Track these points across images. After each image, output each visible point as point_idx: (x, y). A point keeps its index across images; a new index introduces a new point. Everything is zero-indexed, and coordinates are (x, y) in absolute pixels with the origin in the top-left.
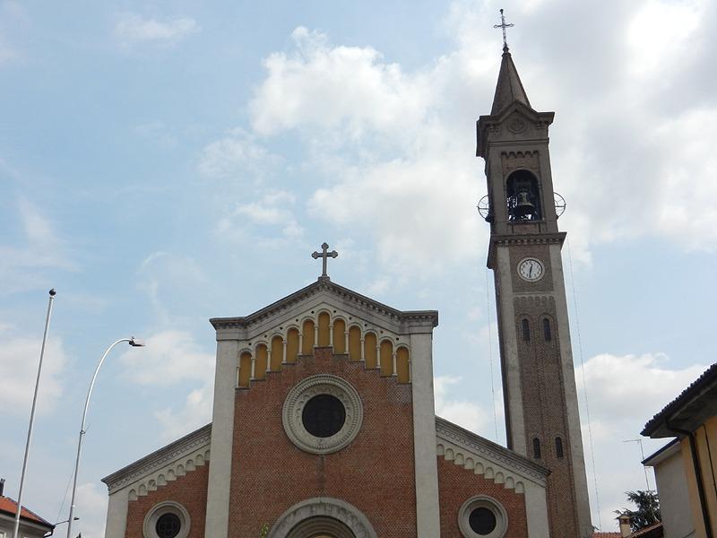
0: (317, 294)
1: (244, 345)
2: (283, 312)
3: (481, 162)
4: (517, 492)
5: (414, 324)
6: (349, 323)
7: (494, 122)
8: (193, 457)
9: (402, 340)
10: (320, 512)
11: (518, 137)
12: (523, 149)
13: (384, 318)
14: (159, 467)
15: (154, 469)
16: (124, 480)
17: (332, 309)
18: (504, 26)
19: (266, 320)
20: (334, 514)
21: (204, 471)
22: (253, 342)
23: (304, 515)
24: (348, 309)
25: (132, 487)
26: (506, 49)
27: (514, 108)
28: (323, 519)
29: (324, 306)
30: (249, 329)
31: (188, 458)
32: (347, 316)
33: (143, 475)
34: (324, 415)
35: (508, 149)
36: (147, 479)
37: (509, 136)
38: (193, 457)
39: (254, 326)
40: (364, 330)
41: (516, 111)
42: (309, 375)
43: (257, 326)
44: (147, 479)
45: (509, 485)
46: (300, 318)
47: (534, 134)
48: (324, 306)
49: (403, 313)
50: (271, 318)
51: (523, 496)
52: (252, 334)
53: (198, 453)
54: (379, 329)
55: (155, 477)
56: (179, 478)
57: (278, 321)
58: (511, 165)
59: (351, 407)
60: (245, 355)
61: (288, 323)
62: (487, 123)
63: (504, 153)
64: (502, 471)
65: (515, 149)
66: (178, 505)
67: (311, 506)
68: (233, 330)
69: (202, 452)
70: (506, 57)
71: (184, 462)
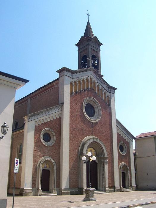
0: (90, 71)
1: (72, 80)
2: (82, 73)
3: (77, 48)
4: (128, 142)
5: (112, 90)
6: (97, 84)
7: (90, 39)
8: (56, 114)
9: (109, 94)
10: (96, 141)
11: (95, 46)
12: (96, 50)
13: (105, 86)
14: (45, 115)
15: (44, 115)
16: (34, 117)
17: (93, 78)
18: (88, 15)
19: (77, 74)
20: (99, 142)
21: (59, 121)
22: (74, 79)
23: (92, 141)
24: (97, 79)
25: (36, 120)
26: (88, 21)
27: (94, 38)
28: (96, 143)
29: (92, 76)
30: (73, 75)
31: (54, 114)
32: (97, 81)
33: (40, 117)
34: (91, 110)
35: (93, 48)
36: (41, 118)
37: (93, 45)
38: (56, 114)
39: (74, 75)
40: (100, 88)
41: (95, 39)
42: (89, 96)
43: (75, 74)
44: (41, 118)
45: (127, 140)
46: (86, 77)
47: (97, 47)
48: (92, 76)
49: (110, 86)
50: (79, 74)
51: (129, 143)
52: (74, 77)
53: (57, 113)
54: (104, 88)
55: (44, 118)
56: (51, 120)
57: (80, 76)
58: (93, 53)
59: (97, 109)
60: (71, 84)
61: (82, 78)
62: (90, 39)
63: (92, 49)
64: (126, 136)
65: (94, 49)
66: (52, 131)
67: (93, 138)
68: (69, 73)
69: (59, 113)
70: (88, 23)
71: (53, 115)
